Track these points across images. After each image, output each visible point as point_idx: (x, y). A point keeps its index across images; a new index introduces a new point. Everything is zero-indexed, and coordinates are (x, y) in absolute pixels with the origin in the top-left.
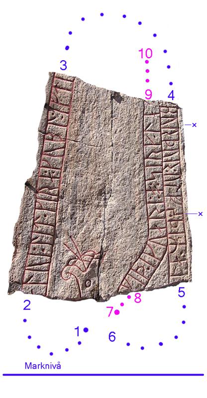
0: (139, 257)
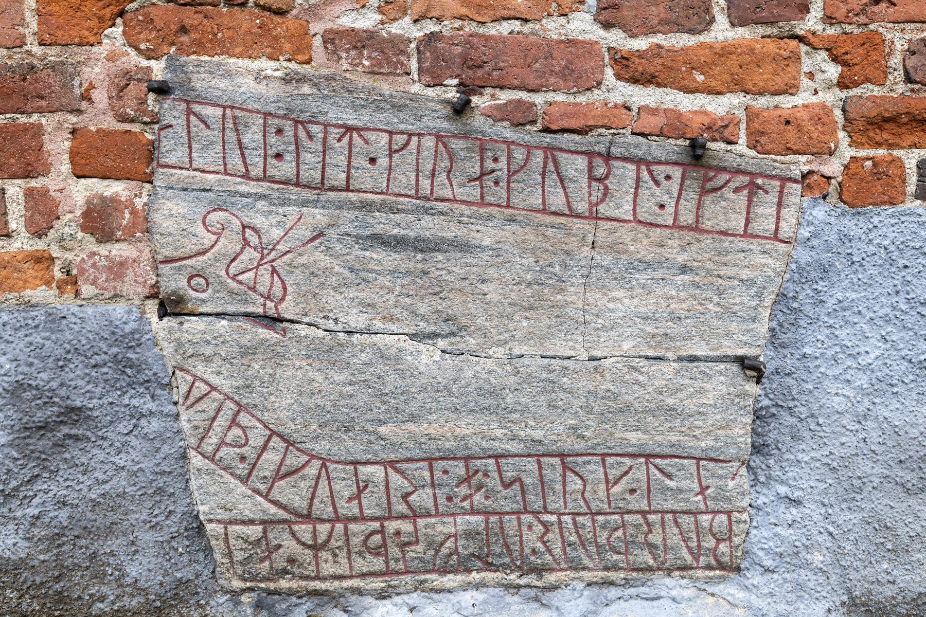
0: (273, 433)
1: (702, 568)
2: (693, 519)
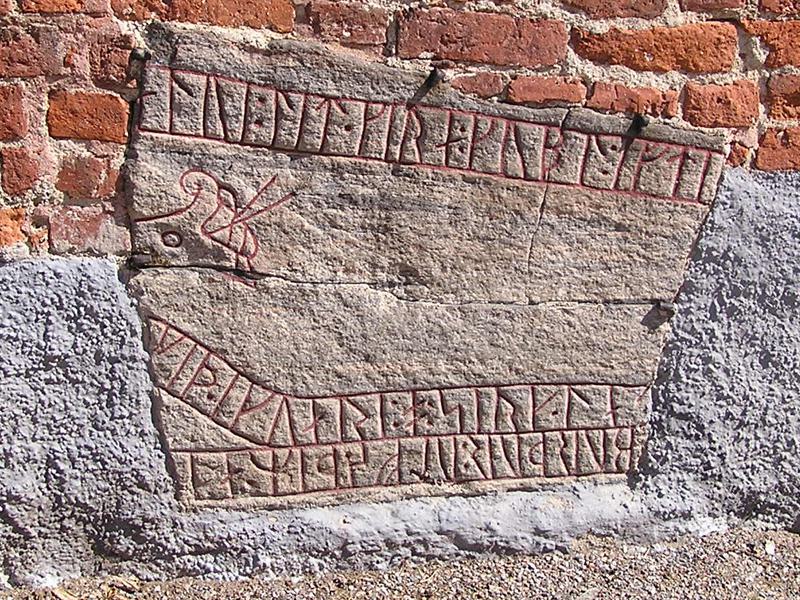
0: (239, 373)
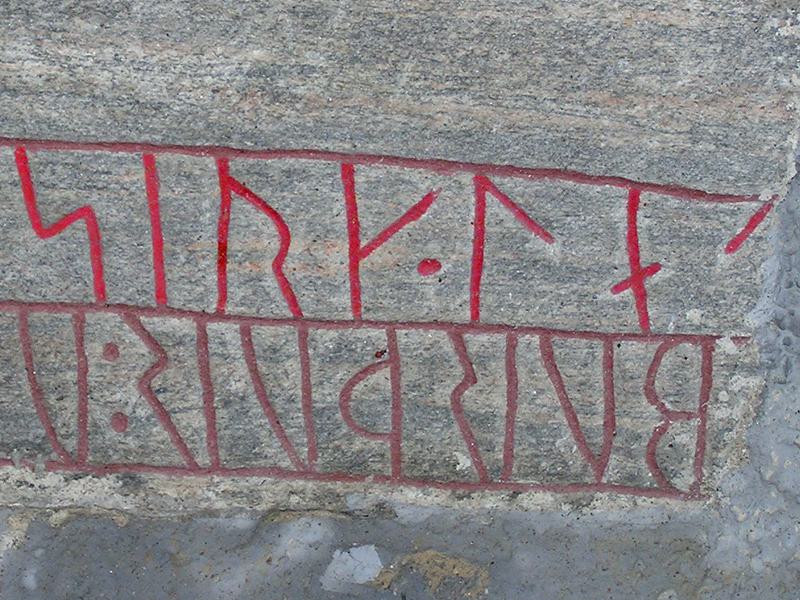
1: (610, 486)
2: (600, 353)
